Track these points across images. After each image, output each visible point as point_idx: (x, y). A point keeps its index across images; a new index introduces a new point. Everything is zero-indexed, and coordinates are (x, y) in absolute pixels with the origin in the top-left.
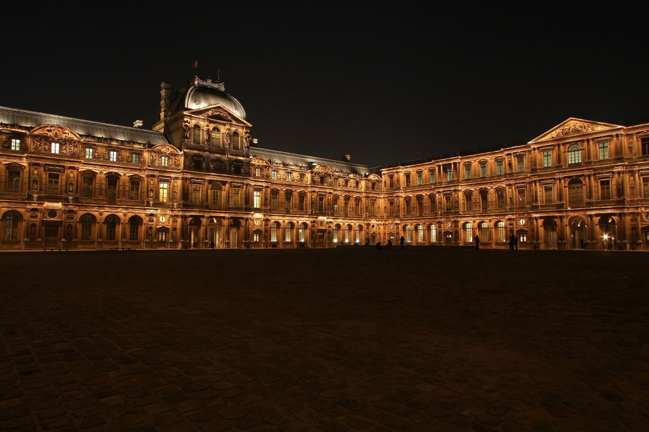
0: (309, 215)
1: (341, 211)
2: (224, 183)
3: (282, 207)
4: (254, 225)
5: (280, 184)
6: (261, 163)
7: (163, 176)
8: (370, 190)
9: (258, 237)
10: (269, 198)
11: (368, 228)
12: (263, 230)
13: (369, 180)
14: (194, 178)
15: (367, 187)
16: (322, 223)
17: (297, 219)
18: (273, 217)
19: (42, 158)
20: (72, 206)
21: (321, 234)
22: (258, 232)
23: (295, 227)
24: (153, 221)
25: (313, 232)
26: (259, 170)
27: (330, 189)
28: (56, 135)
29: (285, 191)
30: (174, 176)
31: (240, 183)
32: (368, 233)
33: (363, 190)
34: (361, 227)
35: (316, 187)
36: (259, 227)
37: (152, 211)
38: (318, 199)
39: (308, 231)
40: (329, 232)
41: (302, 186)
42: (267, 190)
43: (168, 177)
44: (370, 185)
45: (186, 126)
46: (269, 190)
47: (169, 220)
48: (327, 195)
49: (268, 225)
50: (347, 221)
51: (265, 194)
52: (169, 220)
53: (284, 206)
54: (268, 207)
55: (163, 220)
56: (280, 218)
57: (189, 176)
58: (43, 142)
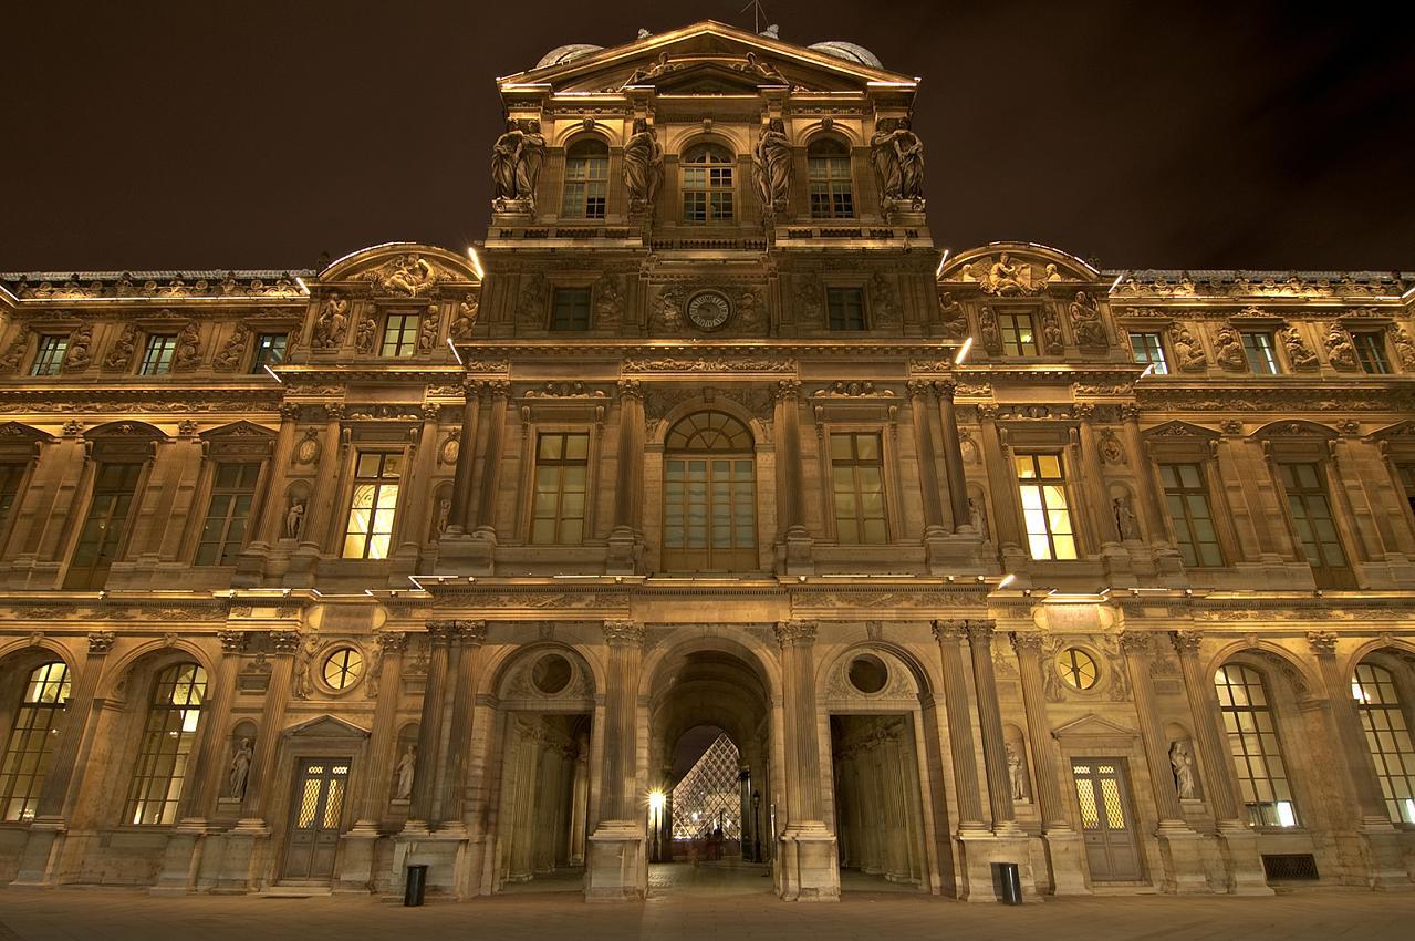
7: (377, 410)
9: (1109, 787)
43: (405, 409)
46: (1126, 433)
52: (377, 674)
56: (1279, 622)
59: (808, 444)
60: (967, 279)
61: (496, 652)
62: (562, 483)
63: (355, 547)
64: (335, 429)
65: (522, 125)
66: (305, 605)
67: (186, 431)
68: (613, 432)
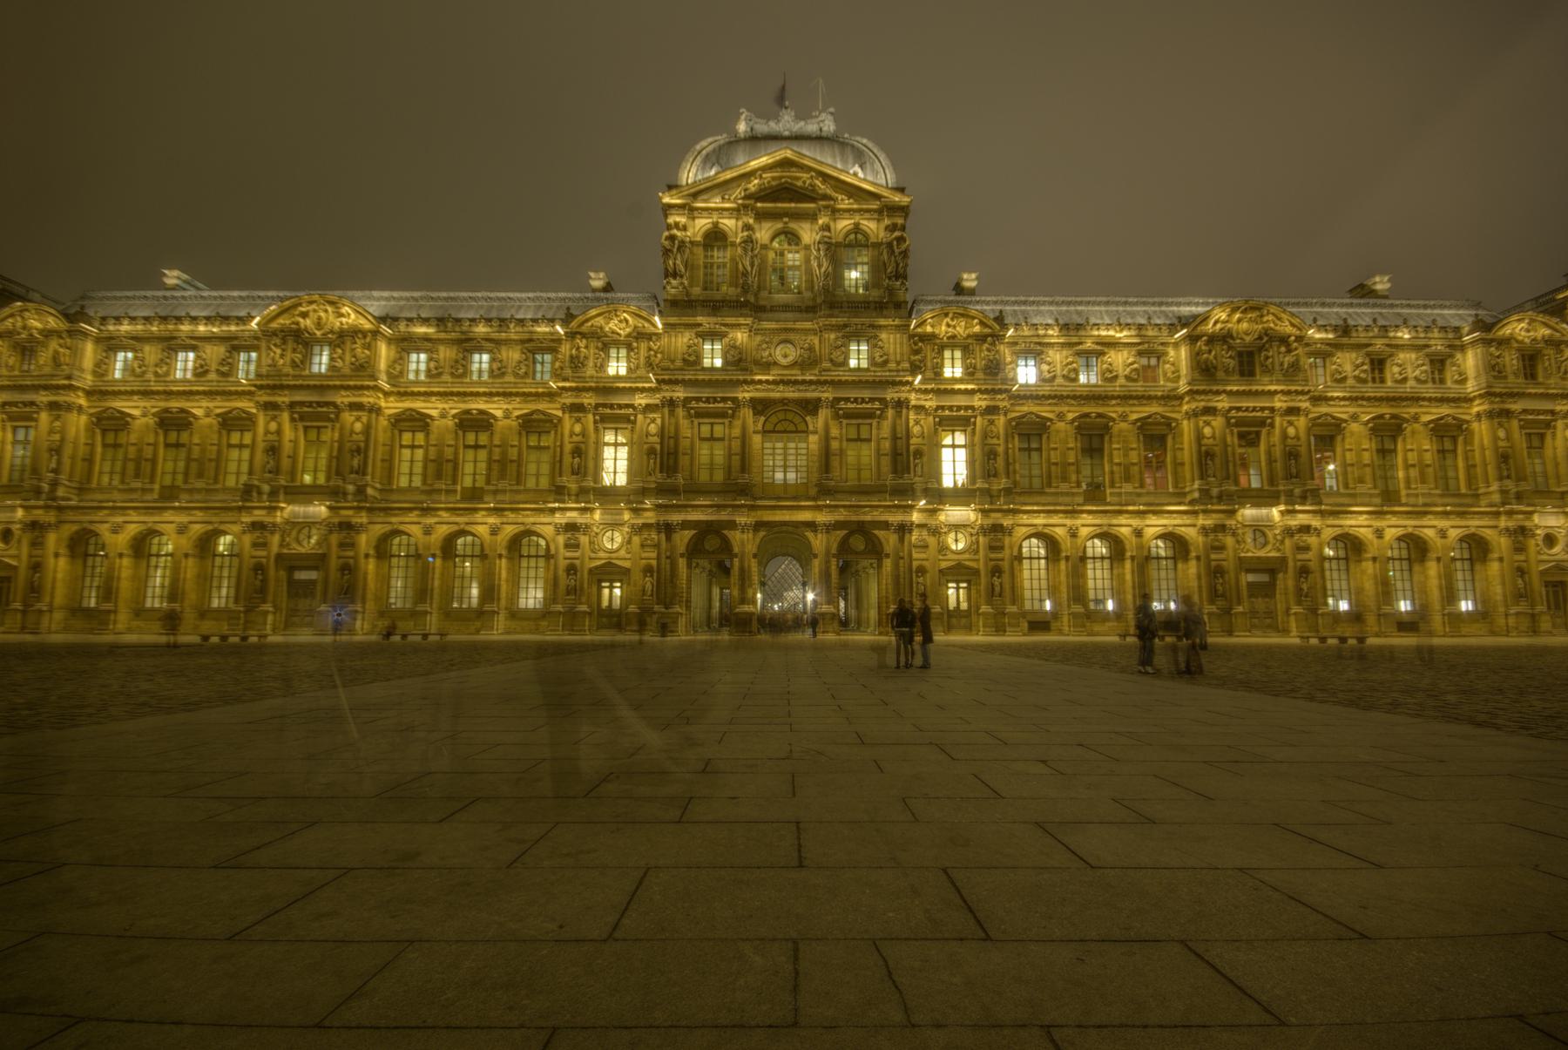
0: (1191, 503)
1: (1361, 481)
2: (811, 407)
3: (1065, 479)
4: (943, 549)
5: (1050, 397)
6: (961, 329)
7: (611, 406)
8: (1515, 382)
10: (1001, 449)
11: (1520, 549)
12: (981, 566)
13: (1504, 342)
14: (698, 399)
15: (1494, 369)
16: (1259, 529)
17: (1135, 522)
18: (1025, 519)
19: (282, 387)
20: (350, 512)
21: (1264, 578)
22: (960, 572)
23: (1128, 554)
24: (577, 546)
25: (1216, 572)
26: (958, 354)
27: (1289, 393)
28: (319, 325)
29: (1073, 420)
30: (644, 402)
31: (872, 400)
32: (1521, 572)
33: (1471, 387)
34: (1477, 548)
35: (1218, 393)
36: (967, 556)
37: (573, 516)
38: (1233, 440)
39: (1192, 568)
40: (1304, 571)
41: (1150, 398)
42: (992, 422)
43: (628, 406)
44: (1511, 360)
45: (672, 238)
46: (1001, 421)
47: (629, 542)
48: (1278, 420)
49: (1002, 548)
50: (1394, 520)
51: (985, 435)
52: (629, 542)
53: (1074, 477)
54: (996, 481)
55: (613, 541)
56: (1055, 520)
57: (680, 393)
58: (290, 345)
59: (834, 432)
60: (929, 329)
61: (688, 534)
62: (712, 449)
63: (607, 480)
64: (590, 416)
65: (677, 225)
66: (591, 510)
67: (507, 415)
68: (738, 423)
